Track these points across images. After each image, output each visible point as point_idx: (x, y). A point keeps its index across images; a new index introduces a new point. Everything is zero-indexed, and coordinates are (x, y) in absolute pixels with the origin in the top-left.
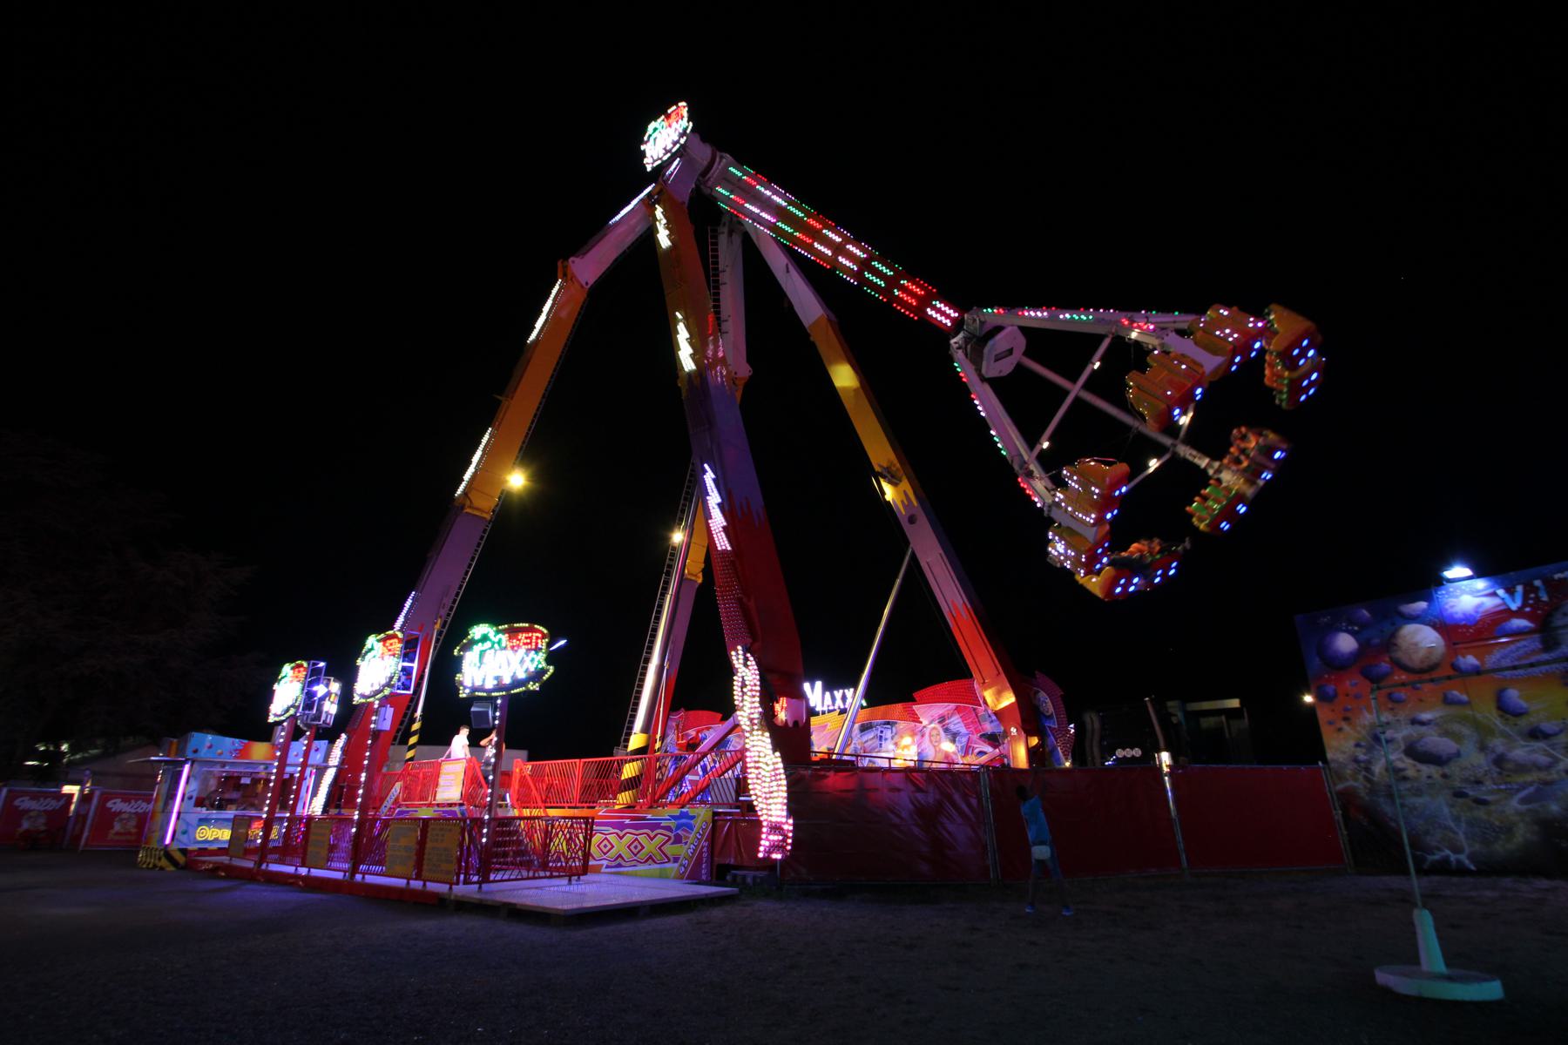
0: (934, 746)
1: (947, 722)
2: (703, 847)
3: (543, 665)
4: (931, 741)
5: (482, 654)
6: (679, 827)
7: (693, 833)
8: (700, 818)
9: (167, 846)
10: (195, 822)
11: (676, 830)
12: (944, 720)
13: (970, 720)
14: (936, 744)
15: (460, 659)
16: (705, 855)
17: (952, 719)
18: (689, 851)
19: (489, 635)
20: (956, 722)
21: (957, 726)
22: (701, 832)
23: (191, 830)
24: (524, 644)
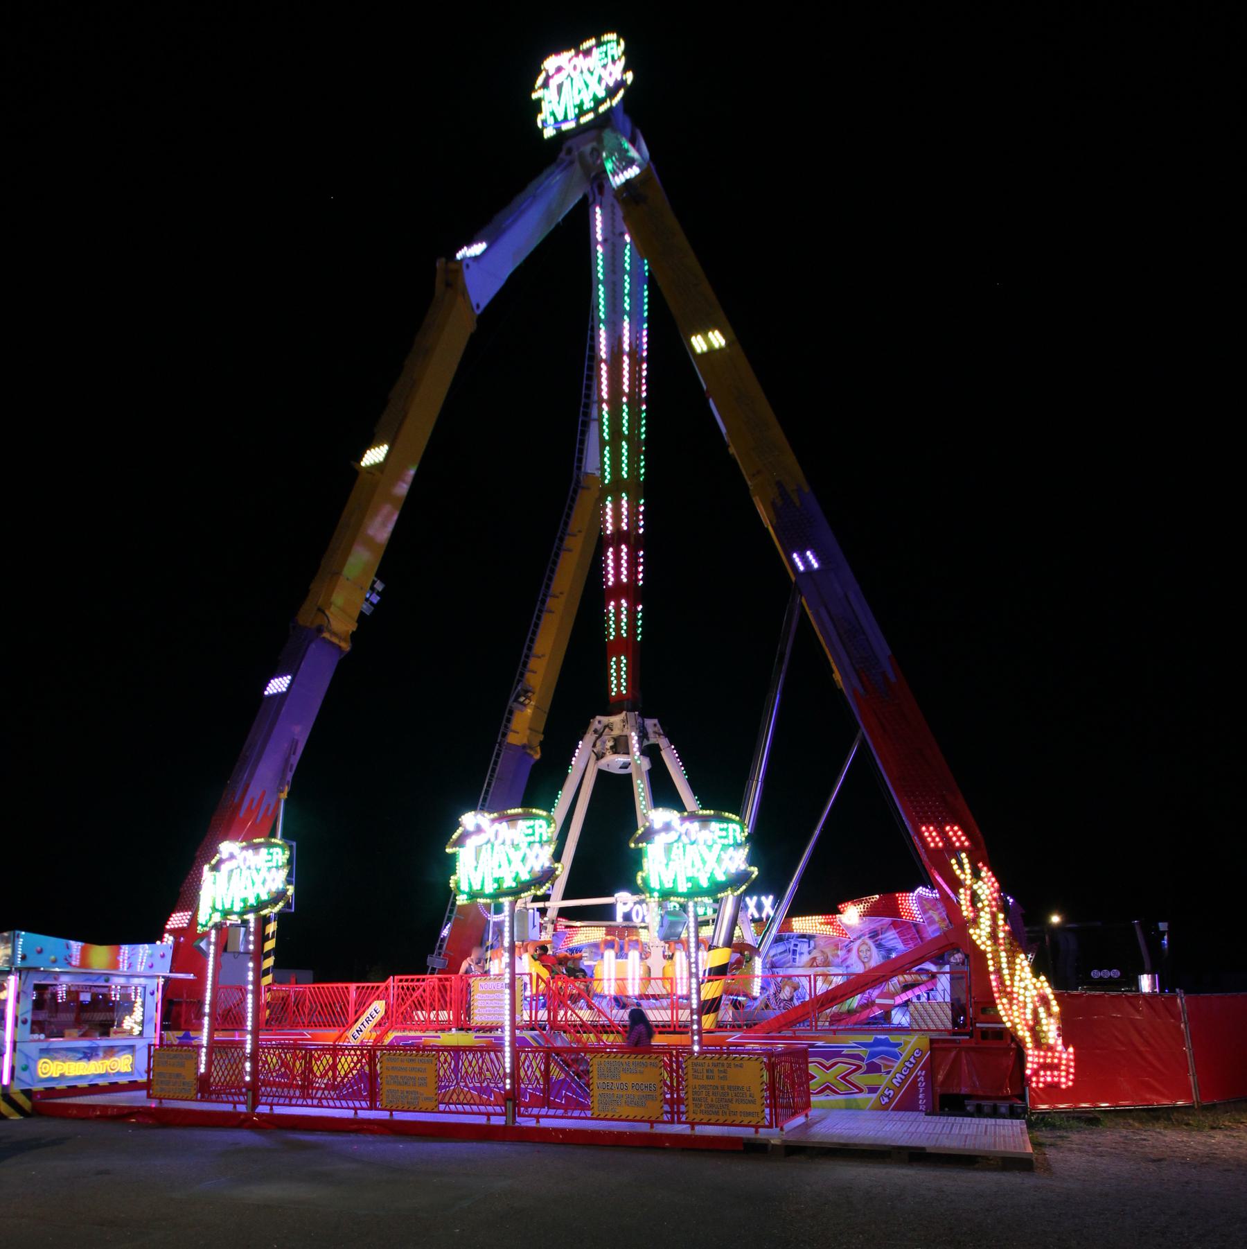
0: (863, 962)
1: (880, 937)
2: (917, 1077)
3: (743, 867)
4: (859, 957)
5: (668, 848)
6: (872, 1055)
7: (899, 1061)
8: (910, 1045)
9: (7, 1086)
10: (35, 1054)
11: (868, 1059)
12: (877, 935)
13: (909, 936)
14: (866, 960)
15: (639, 854)
16: (921, 1085)
17: (886, 935)
18: (894, 1081)
19: (673, 824)
20: (892, 937)
21: (892, 942)
22: (914, 1061)
23: (32, 1064)
24: (721, 837)
